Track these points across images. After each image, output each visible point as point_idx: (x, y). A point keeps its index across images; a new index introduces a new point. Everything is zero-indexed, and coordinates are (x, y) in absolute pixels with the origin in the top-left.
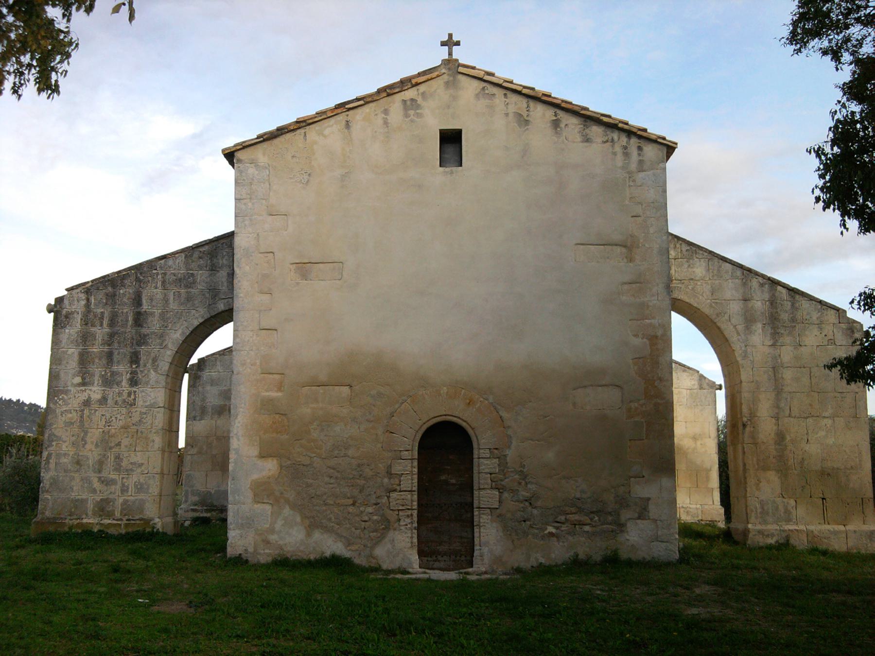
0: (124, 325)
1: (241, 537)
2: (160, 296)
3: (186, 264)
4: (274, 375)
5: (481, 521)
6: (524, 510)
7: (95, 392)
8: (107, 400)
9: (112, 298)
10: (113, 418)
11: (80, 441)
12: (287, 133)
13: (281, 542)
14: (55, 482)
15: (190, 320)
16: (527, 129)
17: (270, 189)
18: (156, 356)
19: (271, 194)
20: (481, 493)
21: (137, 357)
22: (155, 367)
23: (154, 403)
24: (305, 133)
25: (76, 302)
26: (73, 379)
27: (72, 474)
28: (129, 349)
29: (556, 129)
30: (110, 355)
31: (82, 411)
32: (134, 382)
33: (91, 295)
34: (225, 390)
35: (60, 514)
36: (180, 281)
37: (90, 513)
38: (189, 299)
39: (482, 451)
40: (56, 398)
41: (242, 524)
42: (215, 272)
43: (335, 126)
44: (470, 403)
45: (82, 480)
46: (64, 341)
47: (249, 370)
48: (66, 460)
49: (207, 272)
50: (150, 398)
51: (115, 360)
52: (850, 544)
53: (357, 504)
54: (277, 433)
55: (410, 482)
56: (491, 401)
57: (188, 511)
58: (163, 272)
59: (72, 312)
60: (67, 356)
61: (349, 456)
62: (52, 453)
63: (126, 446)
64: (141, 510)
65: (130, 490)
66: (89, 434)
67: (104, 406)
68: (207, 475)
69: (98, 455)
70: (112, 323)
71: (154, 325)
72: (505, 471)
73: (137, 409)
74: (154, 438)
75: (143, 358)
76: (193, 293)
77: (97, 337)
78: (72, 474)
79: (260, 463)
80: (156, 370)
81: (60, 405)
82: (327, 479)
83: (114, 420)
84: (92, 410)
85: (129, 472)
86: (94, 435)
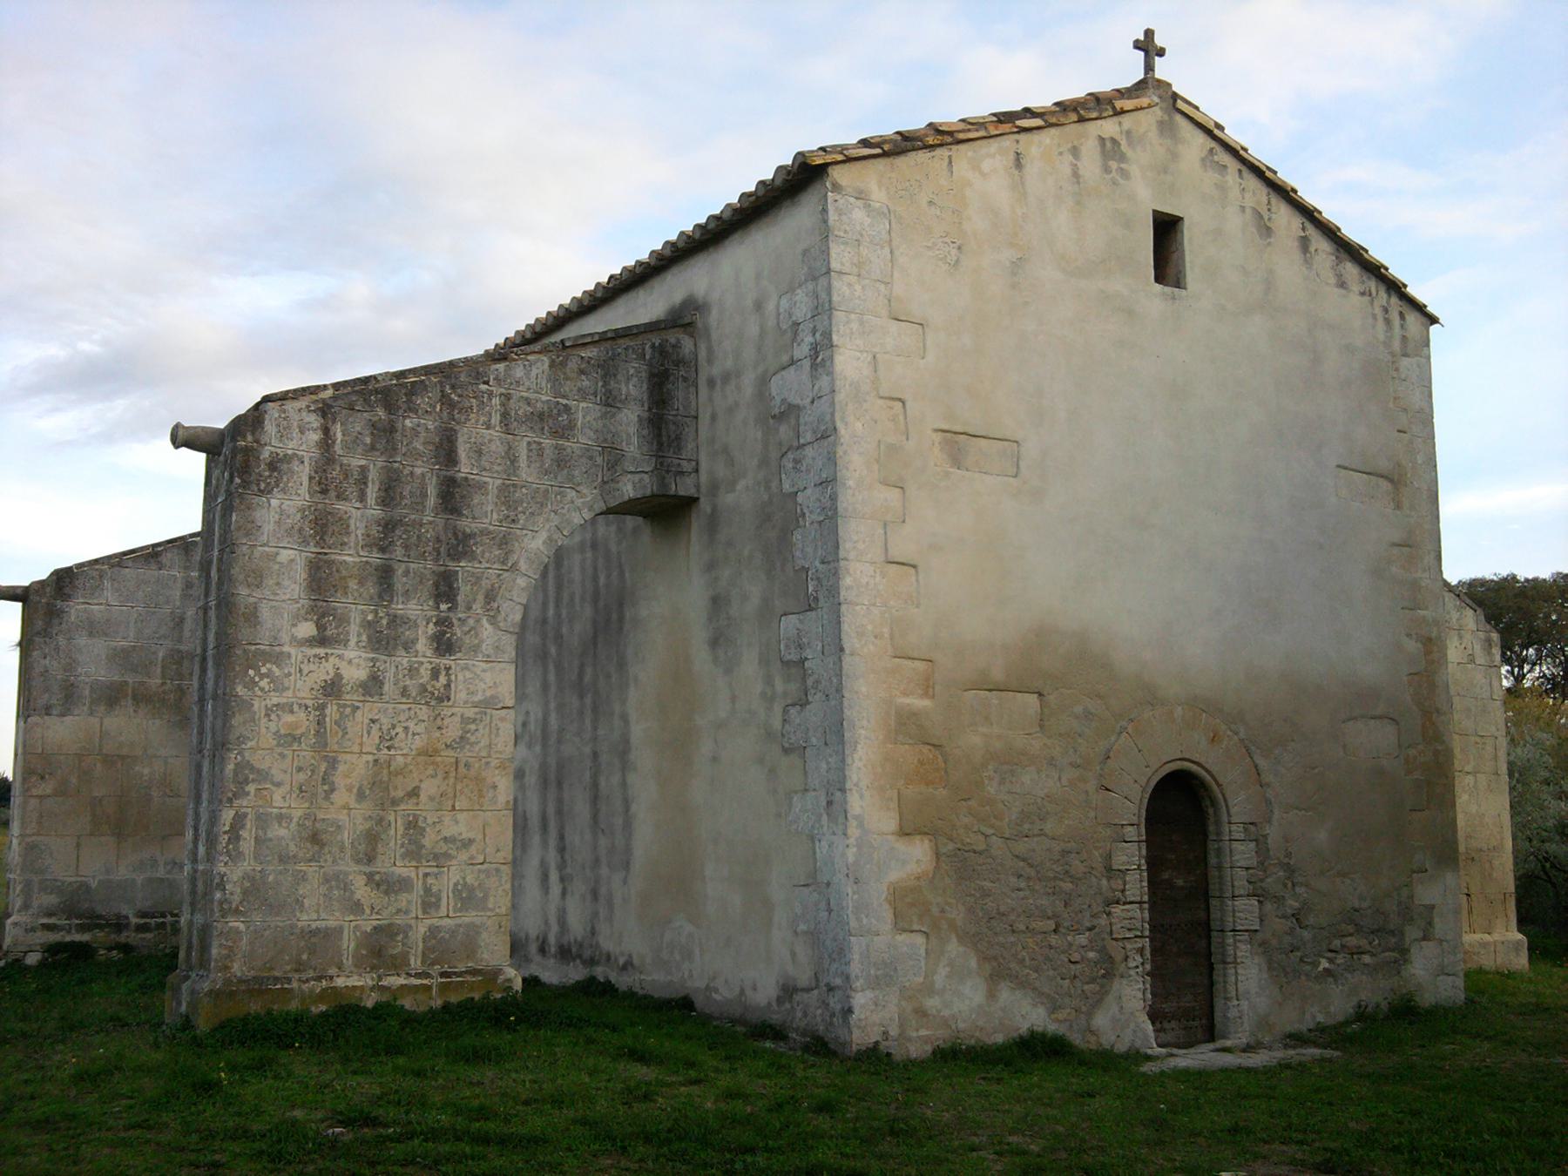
0: (419, 506)
1: (876, 1005)
2: (497, 447)
3: (554, 381)
4: (916, 662)
5: (1239, 954)
6: (1291, 932)
7: (353, 663)
8: (382, 683)
9: (385, 434)
10: (399, 729)
11: (319, 785)
12: (921, 149)
13: (946, 1013)
14: (255, 888)
15: (564, 511)
16: (1269, 244)
17: (892, 261)
18: (492, 585)
19: (896, 274)
20: (1236, 903)
21: (451, 587)
22: (492, 613)
23: (493, 697)
24: (950, 157)
25: (295, 432)
26: (294, 625)
27: (302, 867)
28: (430, 565)
29: (1305, 254)
30: (385, 575)
31: (321, 708)
32: (444, 644)
33: (334, 421)
34: (123, 650)
35: (272, 969)
36: (542, 420)
37: (348, 962)
38: (561, 462)
39: (1234, 827)
40: (251, 672)
41: (877, 977)
42: (613, 410)
43: (998, 157)
44: (1214, 739)
45: (327, 881)
46: (268, 528)
47: (872, 647)
48: (282, 832)
49: (598, 407)
50: (483, 686)
51: (398, 587)
52: (1499, 961)
53: (1061, 929)
54: (927, 784)
55: (1137, 886)
56: (1242, 735)
57: (33, 930)
58: (503, 391)
59: (285, 455)
60: (277, 567)
61: (1046, 835)
62: (245, 815)
63: (431, 799)
64: (471, 948)
65: (444, 902)
66: (341, 768)
67: (376, 698)
68: (78, 845)
69: (366, 819)
70: (388, 497)
71: (484, 514)
72: (1266, 864)
73: (454, 710)
74: (495, 779)
75: (464, 590)
76: (569, 450)
77: (352, 527)
78: (302, 867)
79: (901, 846)
80: (493, 621)
81: (262, 689)
82: (1013, 880)
83: (402, 735)
84: (345, 706)
85: (440, 859)
86: (354, 768)
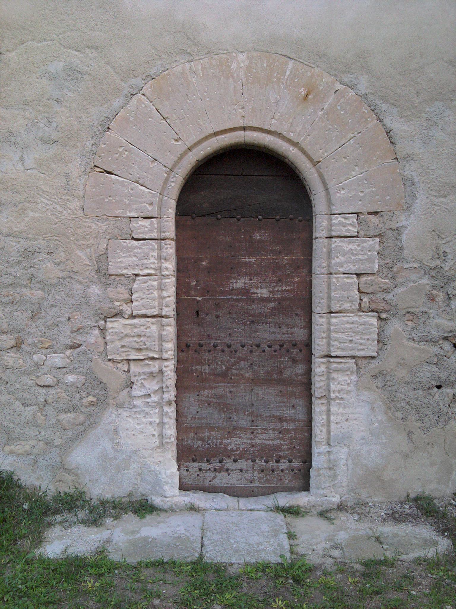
5: (333, 387)
20: (333, 320)
39: (336, 220)
56: (363, 86)
